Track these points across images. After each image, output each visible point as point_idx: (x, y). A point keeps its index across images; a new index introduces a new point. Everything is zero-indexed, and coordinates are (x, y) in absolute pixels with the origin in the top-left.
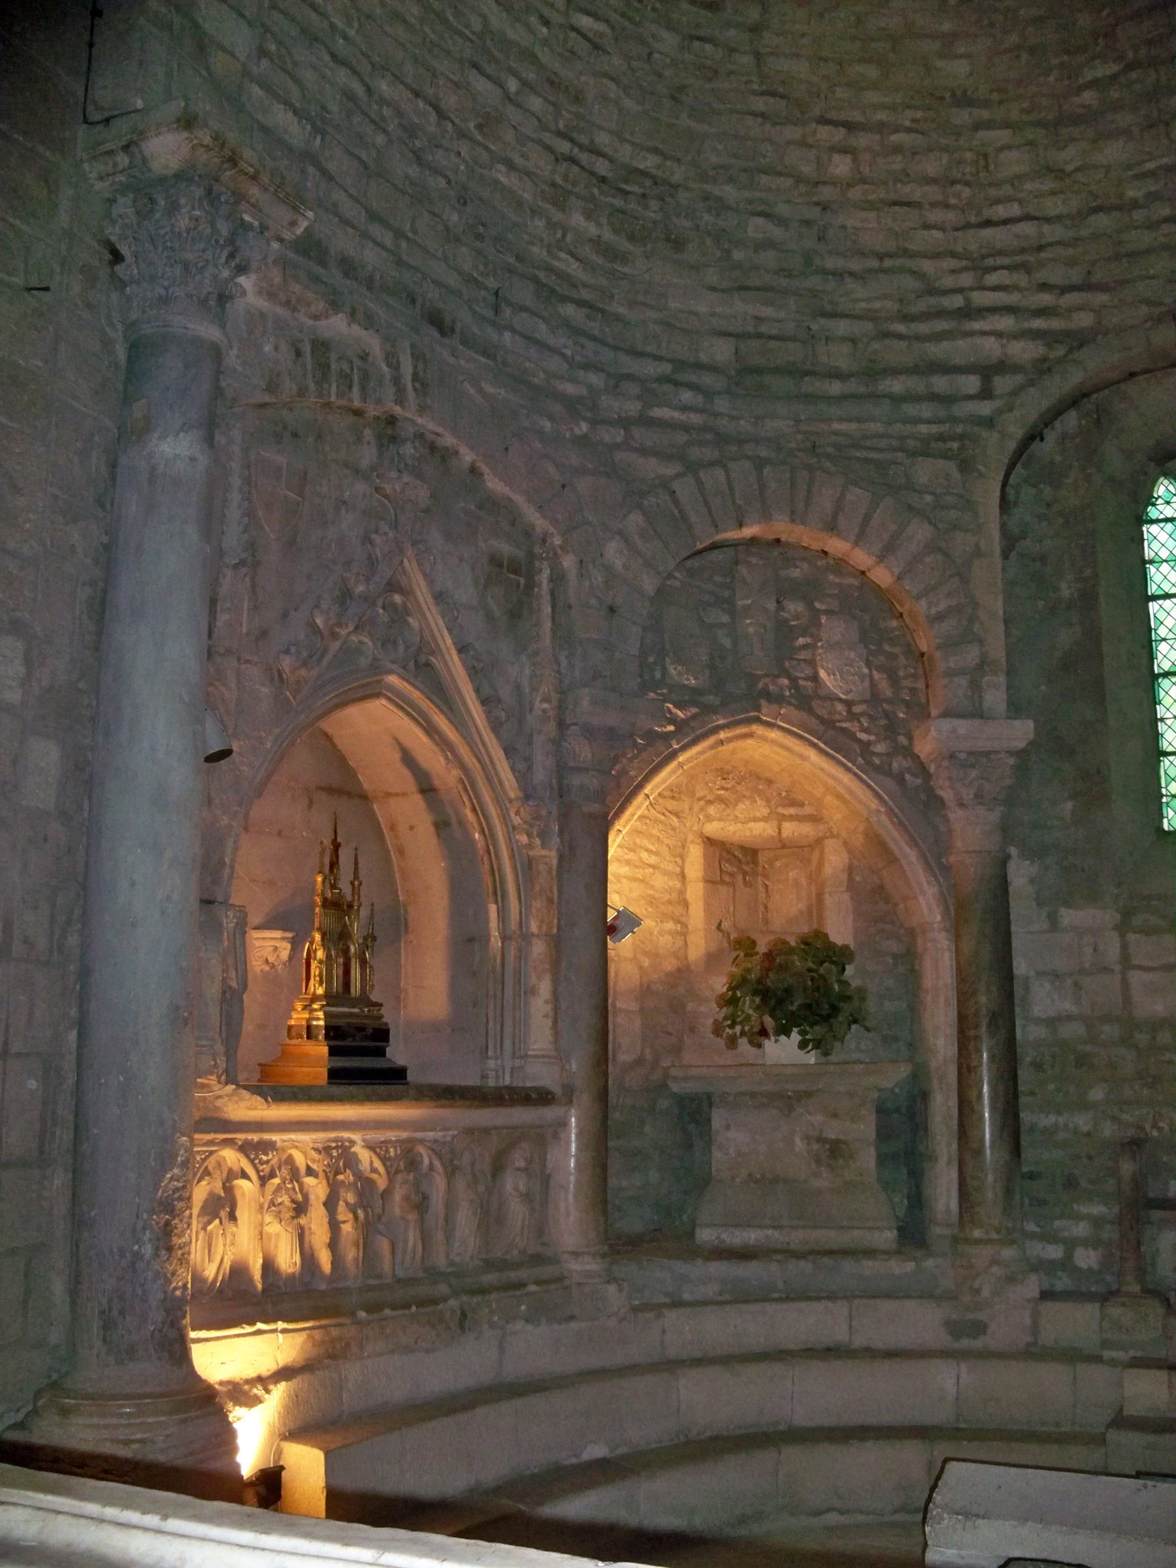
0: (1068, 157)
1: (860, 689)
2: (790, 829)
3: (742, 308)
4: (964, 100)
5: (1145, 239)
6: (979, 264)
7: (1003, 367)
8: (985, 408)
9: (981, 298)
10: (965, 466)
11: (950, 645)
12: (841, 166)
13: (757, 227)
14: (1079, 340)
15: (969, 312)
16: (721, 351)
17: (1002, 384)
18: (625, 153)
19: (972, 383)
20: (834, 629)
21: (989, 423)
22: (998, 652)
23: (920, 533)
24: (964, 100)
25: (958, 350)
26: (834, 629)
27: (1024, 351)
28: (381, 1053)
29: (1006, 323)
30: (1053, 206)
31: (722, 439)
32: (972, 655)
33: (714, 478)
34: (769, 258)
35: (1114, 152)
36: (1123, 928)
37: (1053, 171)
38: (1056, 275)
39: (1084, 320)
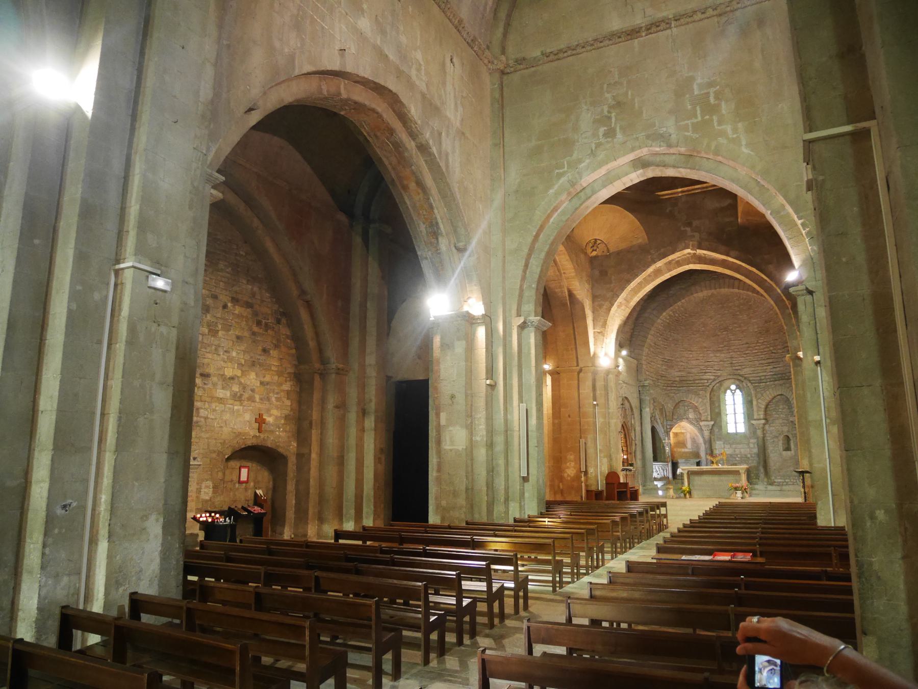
0: (718, 355)
1: (693, 417)
2: (683, 431)
3: (679, 374)
4: (705, 348)
5: (727, 365)
6: (707, 367)
7: (710, 379)
8: (708, 384)
9: (707, 371)
10: (705, 392)
11: (704, 413)
12: (691, 356)
13: (682, 363)
14: (719, 376)
15: (705, 373)
16: (677, 379)
17: (710, 381)
18: (668, 358)
19: (706, 381)
20: (691, 410)
21: (708, 386)
22: (709, 413)
23: (700, 400)
24: (705, 348)
25: (705, 377)
26: (691, 410)
27: (712, 377)
28: (655, 459)
29: (710, 374)
30: (716, 360)
31: (679, 390)
32: (706, 414)
33: (678, 395)
34: (683, 367)
35: (723, 355)
36: (724, 444)
37: (715, 356)
38: (716, 368)
39: (719, 374)
